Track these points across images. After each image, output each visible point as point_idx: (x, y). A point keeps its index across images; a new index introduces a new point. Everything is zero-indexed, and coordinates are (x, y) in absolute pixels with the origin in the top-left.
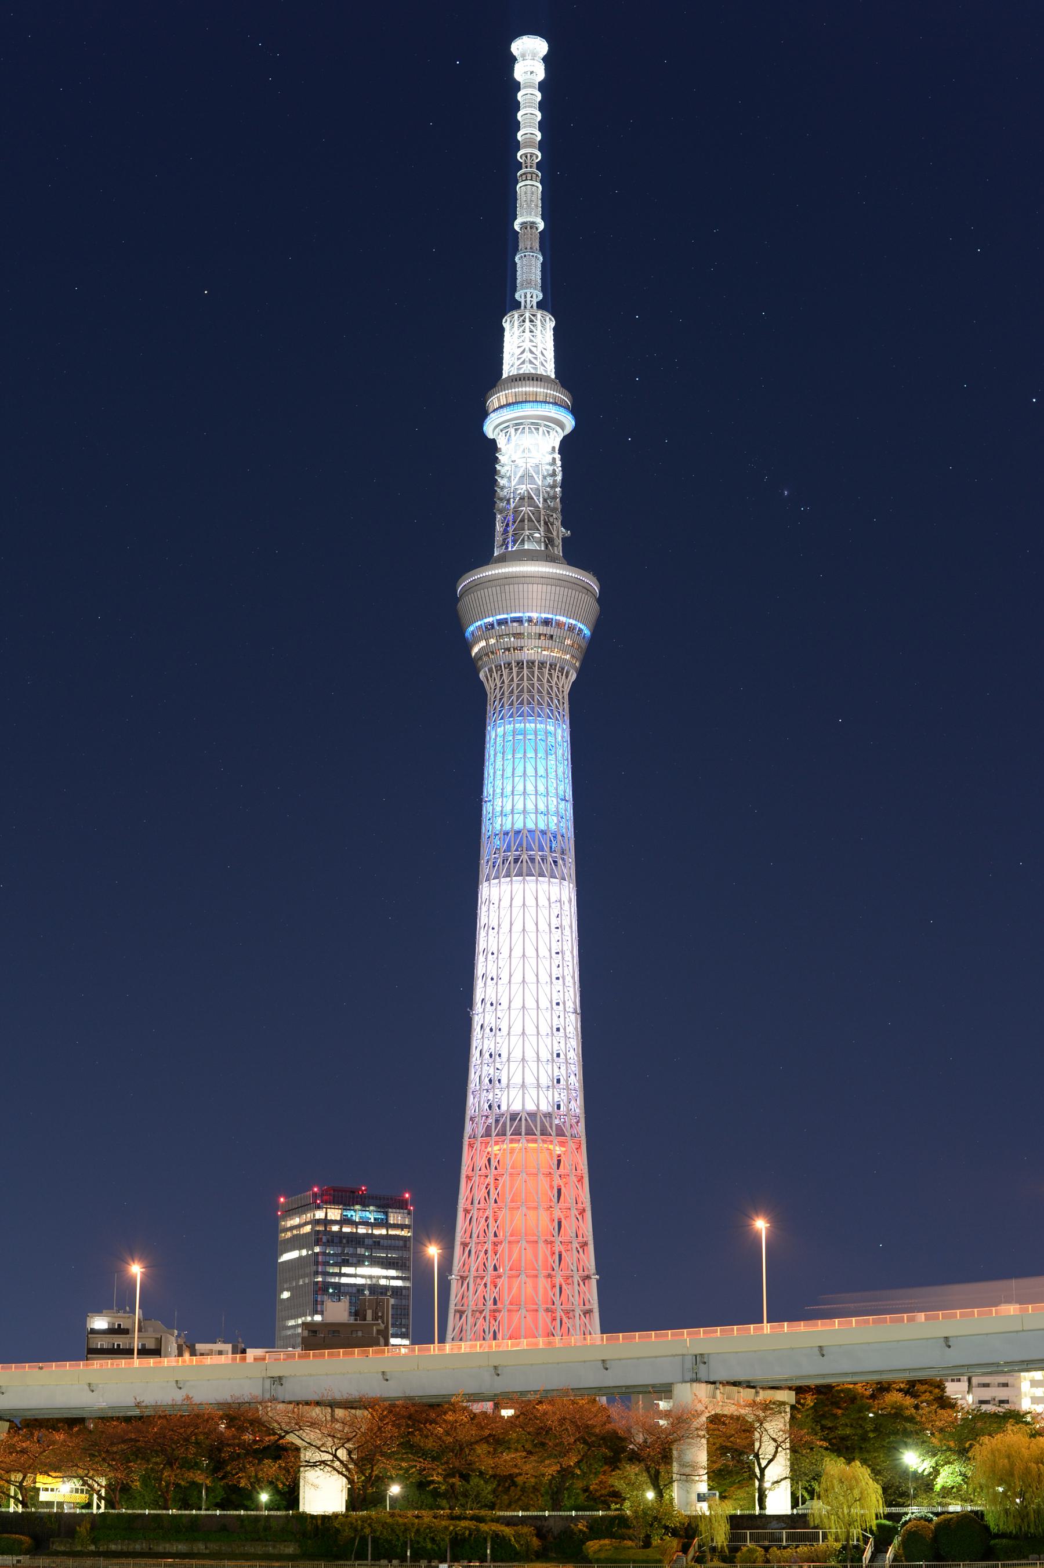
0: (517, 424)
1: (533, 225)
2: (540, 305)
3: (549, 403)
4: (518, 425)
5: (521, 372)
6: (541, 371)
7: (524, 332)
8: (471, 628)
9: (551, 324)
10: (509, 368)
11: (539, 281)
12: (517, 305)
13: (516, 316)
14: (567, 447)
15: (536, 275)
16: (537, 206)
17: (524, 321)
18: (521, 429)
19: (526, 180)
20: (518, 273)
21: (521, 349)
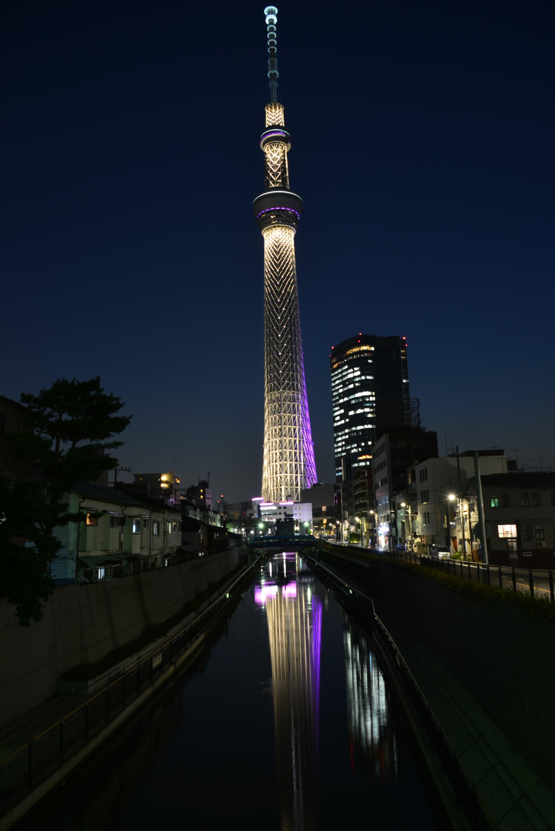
1: (275, 74)
5: (276, 124)
6: (281, 125)
7: (276, 110)
13: (273, 105)
18: (277, 145)
19: (271, 57)
21: (276, 117)
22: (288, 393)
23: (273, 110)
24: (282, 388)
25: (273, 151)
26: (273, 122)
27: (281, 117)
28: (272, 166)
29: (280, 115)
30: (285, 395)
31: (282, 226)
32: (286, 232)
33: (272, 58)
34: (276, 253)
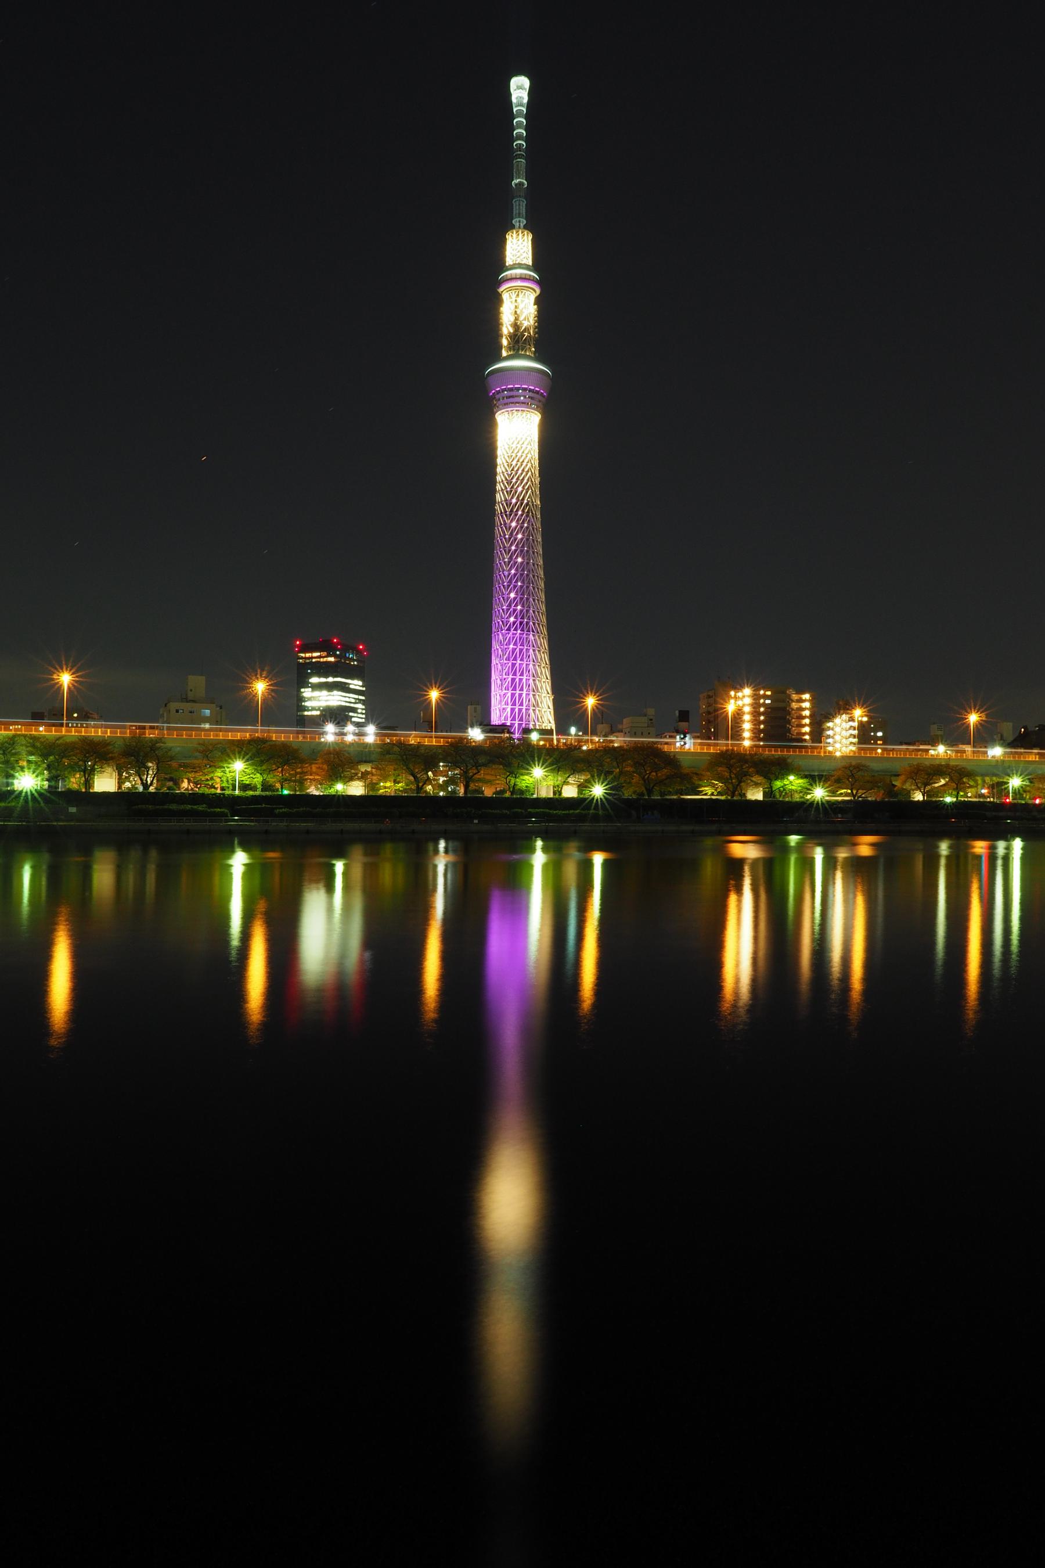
0: (517, 289)
1: (521, 184)
2: (526, 227)
3: (529, 279)
4: (516, 288)
6: (524, 262)
8: (491, 394)
9: (530, 237)
10: (509, 261)
11: (524, 214)
12: (513, 227)
14: (538, 301)
15: (523, 211)
16: (523, 173)
17: (518, 235)
18: (517, 293)
19: (517, 159)
20: (514, 209)
22: (513, 634)
23: (515, 241)
24: (506, 629)
25: (512, 302)
26: (512, 257)
27: (525, 249)
28: (510, 325)
29: (524, 246)
30: (509, 636)
31: (516, 410)
32: (523, 417)
33: (519, 160)
34: (509, 448)
